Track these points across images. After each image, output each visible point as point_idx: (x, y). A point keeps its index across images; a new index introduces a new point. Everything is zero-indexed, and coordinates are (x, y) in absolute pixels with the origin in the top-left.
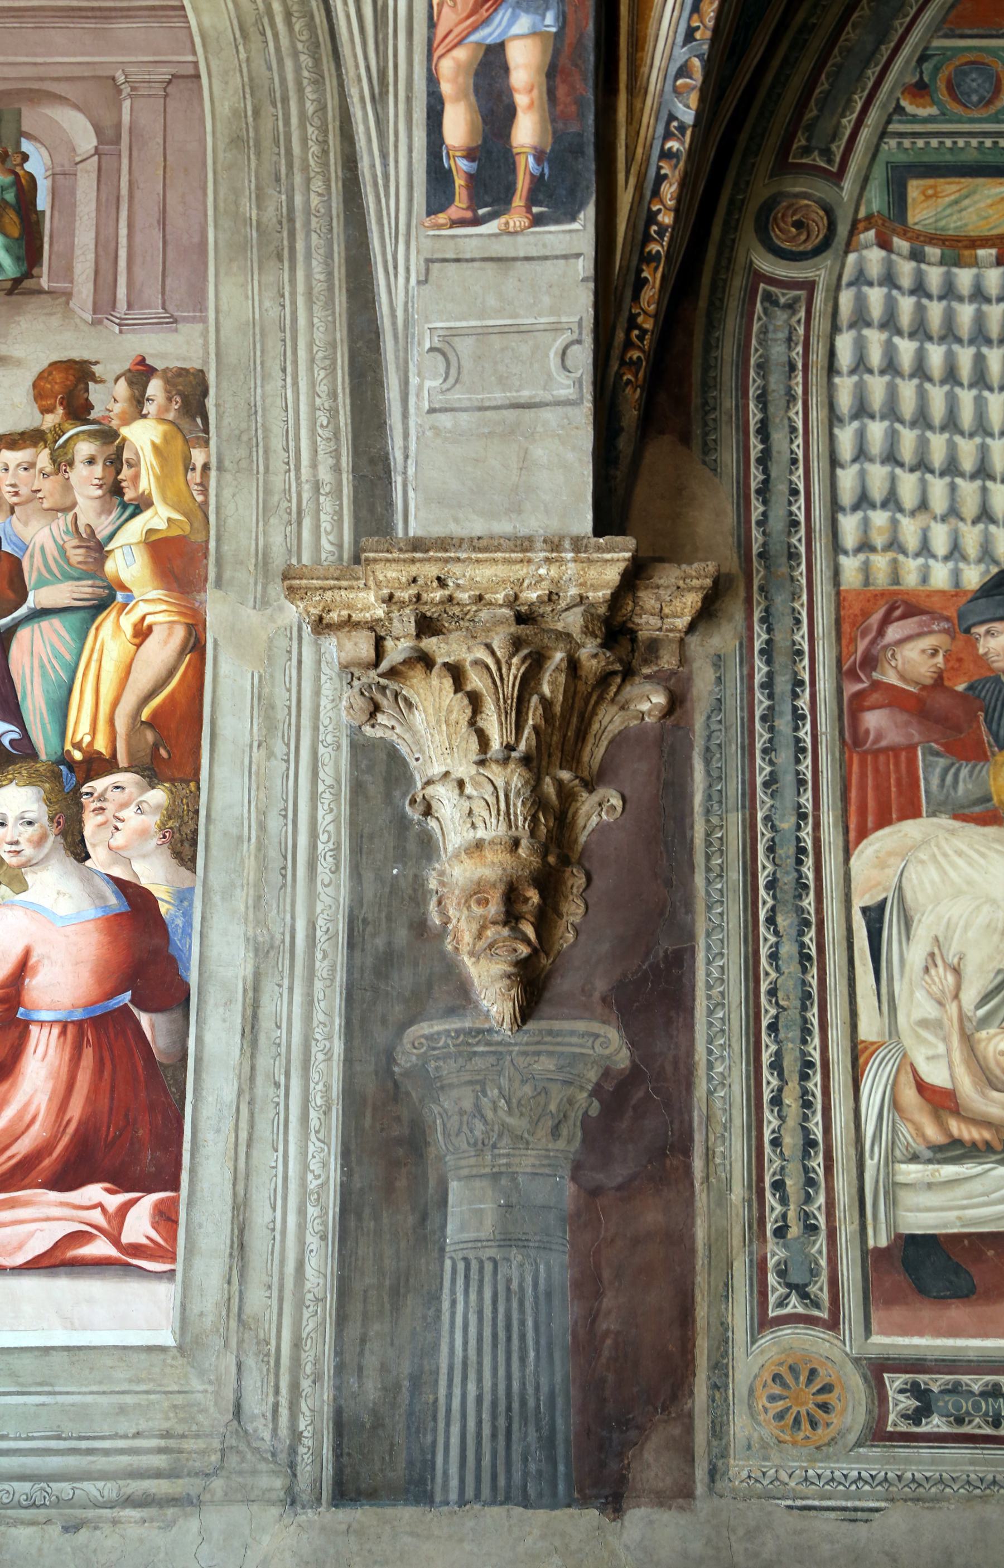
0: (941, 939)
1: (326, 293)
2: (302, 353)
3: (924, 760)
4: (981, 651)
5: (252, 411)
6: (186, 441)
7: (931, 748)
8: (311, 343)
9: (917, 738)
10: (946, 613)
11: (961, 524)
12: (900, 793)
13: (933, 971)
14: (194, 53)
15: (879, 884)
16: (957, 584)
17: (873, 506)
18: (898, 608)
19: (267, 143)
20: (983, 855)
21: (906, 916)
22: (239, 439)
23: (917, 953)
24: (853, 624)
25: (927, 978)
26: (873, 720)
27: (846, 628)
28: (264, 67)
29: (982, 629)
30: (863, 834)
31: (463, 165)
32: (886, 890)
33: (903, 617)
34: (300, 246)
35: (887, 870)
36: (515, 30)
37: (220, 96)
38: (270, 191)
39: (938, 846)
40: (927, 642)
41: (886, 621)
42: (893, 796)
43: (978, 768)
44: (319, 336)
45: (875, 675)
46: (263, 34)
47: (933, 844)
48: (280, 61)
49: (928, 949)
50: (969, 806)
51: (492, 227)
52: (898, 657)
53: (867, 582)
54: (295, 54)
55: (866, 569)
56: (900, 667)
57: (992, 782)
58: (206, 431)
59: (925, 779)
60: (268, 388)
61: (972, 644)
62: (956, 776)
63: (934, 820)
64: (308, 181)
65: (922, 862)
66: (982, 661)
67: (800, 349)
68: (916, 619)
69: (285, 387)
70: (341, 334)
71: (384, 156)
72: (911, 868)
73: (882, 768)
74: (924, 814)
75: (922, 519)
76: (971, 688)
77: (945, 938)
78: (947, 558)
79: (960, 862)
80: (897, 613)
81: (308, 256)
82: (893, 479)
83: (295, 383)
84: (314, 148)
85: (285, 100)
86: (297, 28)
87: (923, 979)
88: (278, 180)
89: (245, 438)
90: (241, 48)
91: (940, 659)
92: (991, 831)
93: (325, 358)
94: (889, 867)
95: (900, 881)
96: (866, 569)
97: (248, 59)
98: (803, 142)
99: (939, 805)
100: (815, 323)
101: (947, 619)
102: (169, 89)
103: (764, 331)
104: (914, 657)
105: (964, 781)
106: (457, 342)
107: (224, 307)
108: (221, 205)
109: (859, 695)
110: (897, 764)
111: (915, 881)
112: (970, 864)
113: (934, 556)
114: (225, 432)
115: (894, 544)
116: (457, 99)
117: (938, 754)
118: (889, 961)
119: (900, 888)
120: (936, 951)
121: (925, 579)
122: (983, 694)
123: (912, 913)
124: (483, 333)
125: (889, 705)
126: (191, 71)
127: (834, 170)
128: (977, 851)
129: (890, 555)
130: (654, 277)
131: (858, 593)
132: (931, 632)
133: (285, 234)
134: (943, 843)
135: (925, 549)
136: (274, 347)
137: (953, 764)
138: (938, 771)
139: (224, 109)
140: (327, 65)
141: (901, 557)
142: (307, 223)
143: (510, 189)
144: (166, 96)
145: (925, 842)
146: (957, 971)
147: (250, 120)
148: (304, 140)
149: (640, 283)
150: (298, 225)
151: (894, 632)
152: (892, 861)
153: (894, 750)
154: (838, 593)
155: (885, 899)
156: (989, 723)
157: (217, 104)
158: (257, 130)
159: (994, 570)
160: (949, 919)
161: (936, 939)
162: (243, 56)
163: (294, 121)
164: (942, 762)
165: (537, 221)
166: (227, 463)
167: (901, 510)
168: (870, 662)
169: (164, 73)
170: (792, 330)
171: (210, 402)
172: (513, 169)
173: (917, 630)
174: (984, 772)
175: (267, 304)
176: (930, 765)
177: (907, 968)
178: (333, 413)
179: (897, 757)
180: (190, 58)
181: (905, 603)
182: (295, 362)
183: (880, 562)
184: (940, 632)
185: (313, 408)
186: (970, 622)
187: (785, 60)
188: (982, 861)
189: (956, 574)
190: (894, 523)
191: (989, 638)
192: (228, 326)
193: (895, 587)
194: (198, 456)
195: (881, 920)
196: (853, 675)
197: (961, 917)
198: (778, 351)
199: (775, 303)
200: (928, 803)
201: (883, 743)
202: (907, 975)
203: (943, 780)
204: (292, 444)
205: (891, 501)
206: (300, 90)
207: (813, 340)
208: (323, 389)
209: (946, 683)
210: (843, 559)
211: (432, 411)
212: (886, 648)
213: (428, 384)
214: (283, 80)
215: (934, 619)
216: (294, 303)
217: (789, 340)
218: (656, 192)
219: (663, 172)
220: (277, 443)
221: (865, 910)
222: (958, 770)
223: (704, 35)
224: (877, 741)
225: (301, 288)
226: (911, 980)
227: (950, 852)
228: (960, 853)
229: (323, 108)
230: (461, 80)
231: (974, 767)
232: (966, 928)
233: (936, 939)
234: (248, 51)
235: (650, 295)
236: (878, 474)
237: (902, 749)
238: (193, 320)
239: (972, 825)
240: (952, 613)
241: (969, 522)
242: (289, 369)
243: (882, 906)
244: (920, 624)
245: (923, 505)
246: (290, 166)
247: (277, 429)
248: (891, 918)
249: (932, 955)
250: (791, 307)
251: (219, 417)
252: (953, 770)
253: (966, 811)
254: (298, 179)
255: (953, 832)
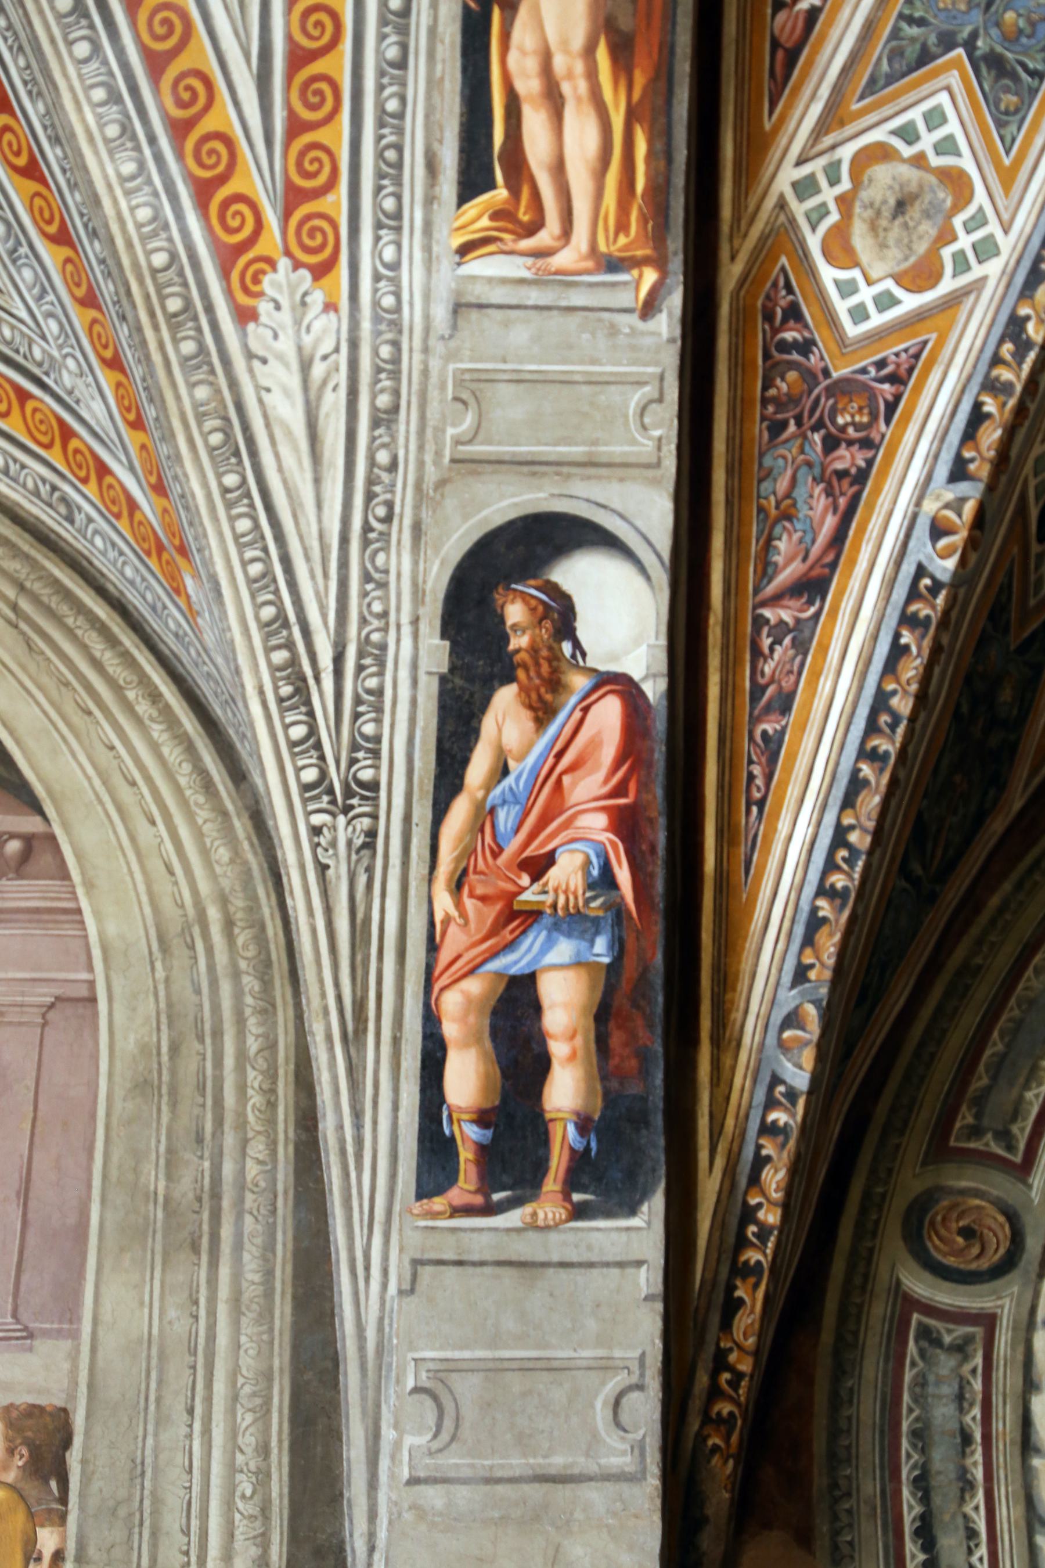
1: (262, 1301)
2: (220, 1387)
5: (137, 1471)
6: (31, 1515)
8: (235, 1372)
14: (90, 968)
19: (187, 1090)
22: (114, 1512)
28: (189, 992)
31: (473, 1132)
34: (226, 1232)
36: (551, 958)
37: (125, 1025)
38: (188, 1156)
44: (248, 1362)
46: (192, 947)
48: (214, 983)
51: (513, 1218)
54: (236, 975)
58: (64, 1500)
60: (164, 1437)
64: (244, 1143)
67: (976, 1411)
69: (190, 1436)
70: (281, 1360)
71: (357, 1115)
81: (238, 1247)
83: (207, 1431)
84: (255, 1099)
85: (217, 1034)
86: (240, 941)
88: (200, 1140)
89: (122, 1512)
90: (158, 965)
93: (254, 1394)
97: (167, 980)
98: (970, 1120)
100: (998, 1374)
102: (51, 1015)
103: (921, 1382)
106: (456, 1381)
107: (106, 1316)
108: (114, 1173)
114: (93, 1502)
116: (465, 1045)
124: (495, 1369)
126: (83, 992)
127: (1018, 1159)
130: (753, 1297)
133: (206, 1215)
136: (178, 1377)
139: (128, 1044)
140: (281, 989)
142: (240, 1200)
143: (540, 1168)
144: (44, 1025)
147: (165, 1058)
148: (242, 1088)
149: (732, 1306)
150: (226, 1203)
157: (118, 1036)
158: (173, 1072)
162: (160, 974)
163: (229, 1062)
165: (579, 1212)
166: (92, 1551)
169: (44, 995)
170: (963, 1385)
171: (74, 1458)
172: (544, 1140)
175: (172, 1313)
178: (262, 1477)
180: (85, 976)
182: (208, 1400)
185: (232, 1469)
187: (939, 1009)
192: (109, 1342)
194: (47, 1540)
198: (943, 1413)
199: (937, 1343)
204: (195, 1523)
206: (240, 1021)
207: (997, 1400)
208: (248, 1440)
211: (414, 1481)
213: (409, 1440)
214: (216, 1008)
216: (212, 1313)
217: (960, 1397)
218: (754, 1179)
219: (764, 1152)
220: (172, 1521)
223: (821, 975)
225: (224, 1291)
229: (271, 1046)
230: (472, 1019)
234: (168, 969)
235: (747, 1323)
238: (59, 1334)
242: (198, 1410)
246: (219, 1122)
247: (174, 1500)
250: (961, 1349)
251: (86, 1479)
254: (230, 1140)
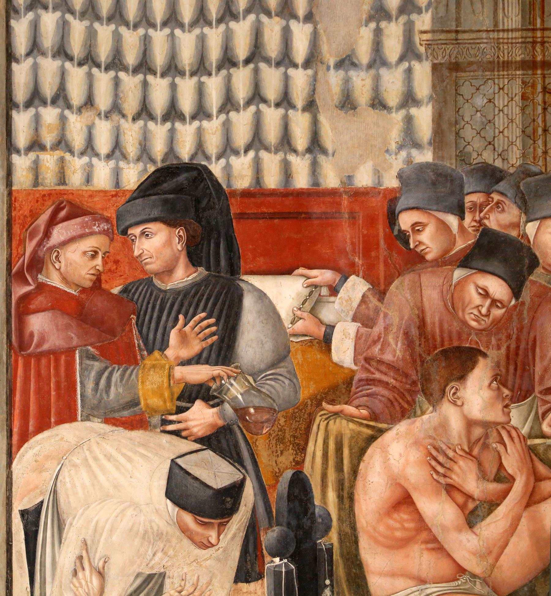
0: (89, 543)
3: (81, 364)
4: (136, 253)
7: (88, 351)
9: (75, 341)
10: (107, 214)
11: (122, 121)
12: (58, 396)
13: (80, 574)
15: (36, 487)
16: (117, 184)
17: (44, 103)
18: (63, 208)
20: (129, 460)
21: (59, 520)
23: (67, 557)
24: (23, 225)
25: (75, 580)
26: (38, 323)
27: (16, 229)
29: (136, 231)
30: (24, 438)
32: (42, 493)
33: (67, 218)
35: (44, 474)
39: (89, 449)
40: (88, 244)
41: (52, 222)
42: (53, 399)
43: (129, 372)
45: (41, 278)
47: (85, 447)
49: (77, 552)
50: (119, 410)
52: (62, 259)
53: (36, 183)
55: (36, 168)
56: (62, 269)
57: (140, 387)
59: (82, 383)
61: (128, 245)
62: (109, 379)
63: (88, 424)
65: (75, 466)
66: (136, 263)
68: (79, 220)
72: (65, 473)
73: (43, 372)
74: (79, 418)
75: (88, 115)
76: (125, 290)
77: (93, 541)
78: (109, 157)
79: (109, 466)
80: (63, 214)
82: (63, 74)
87: (71, 582)
91: (99, 261)
92: (137, 435)
94: (46, 470)
95: (55, 484)
96: (36, 168)
99: (93, 409)
101: (107, 220)
104: (76, 260)
105: (116, 385)
109: (25, 298)
110: (57, 367)
111: (68, 485)
112: (117, 468)
113: (97, 155)
115: (62, 143)
117: (93, 358)
118: (43, 565)
119: (55, 492)
120: (84, 554)
121: (88, 179)
122: (136, 297)
123: (65, 516)
125: (52, 308)
128: (124, 455)
129: (58, 154)
131: (28, 193)
132: (92, 234)
134: (95, 447)
135: (89, 147)
137: (106, 368)
138: (93, 374)
141: (68, 156)
145: (79, 446)
146: (101, 574)
151: (59, 233)
152: (48, 464)
153: (55, 353)
154: (10, 194)
155: (42, 502)
156: (140, 326)
159: (151, 169)
160: (97, 522)
161: (85, 543)
164: (97, 365)
167: (69, 106)
168: (37, 264)
173: (80, 232)
174: (133, 376)
176: (86, 369)
177: (58, 571)
179: (57, 361)
181: (71, 204)
183: (49, 160)
184: (100, 233)
186: (128, 223)
188: (128, 466)
189: (117, 173)
190: (63, 119)
191: (144, 239)
193: (62, 187)
195: (37, 524)
196: (21, 277)
197: (107, 520)
200: (83, 407)
201: (46, 347)
202: (57, 578)
203: (97, 384)
205: (61, 97)
209: (104, 286)
210: (15, 158)
212: (51, 249)
215: (95, 220)
221: (23, 513)
222: (111, 374)
224: (39, 345)
226: (61, 582)
227: (101, 457)
228: (109, 457)
231: (125, 371)
232: (112, 531)
233: (85, 543)
236: (49, 67)
237: (62, 353)
239: (121, 429)
240: (111, 213)
241: (130, 118)
243: (38, 509)
244: (83, 226)
245: (90, 101)
248: (46, 520)
249: (81, 558)
252: (106, 374)
253: (117, 415)
255: (103, 436)
